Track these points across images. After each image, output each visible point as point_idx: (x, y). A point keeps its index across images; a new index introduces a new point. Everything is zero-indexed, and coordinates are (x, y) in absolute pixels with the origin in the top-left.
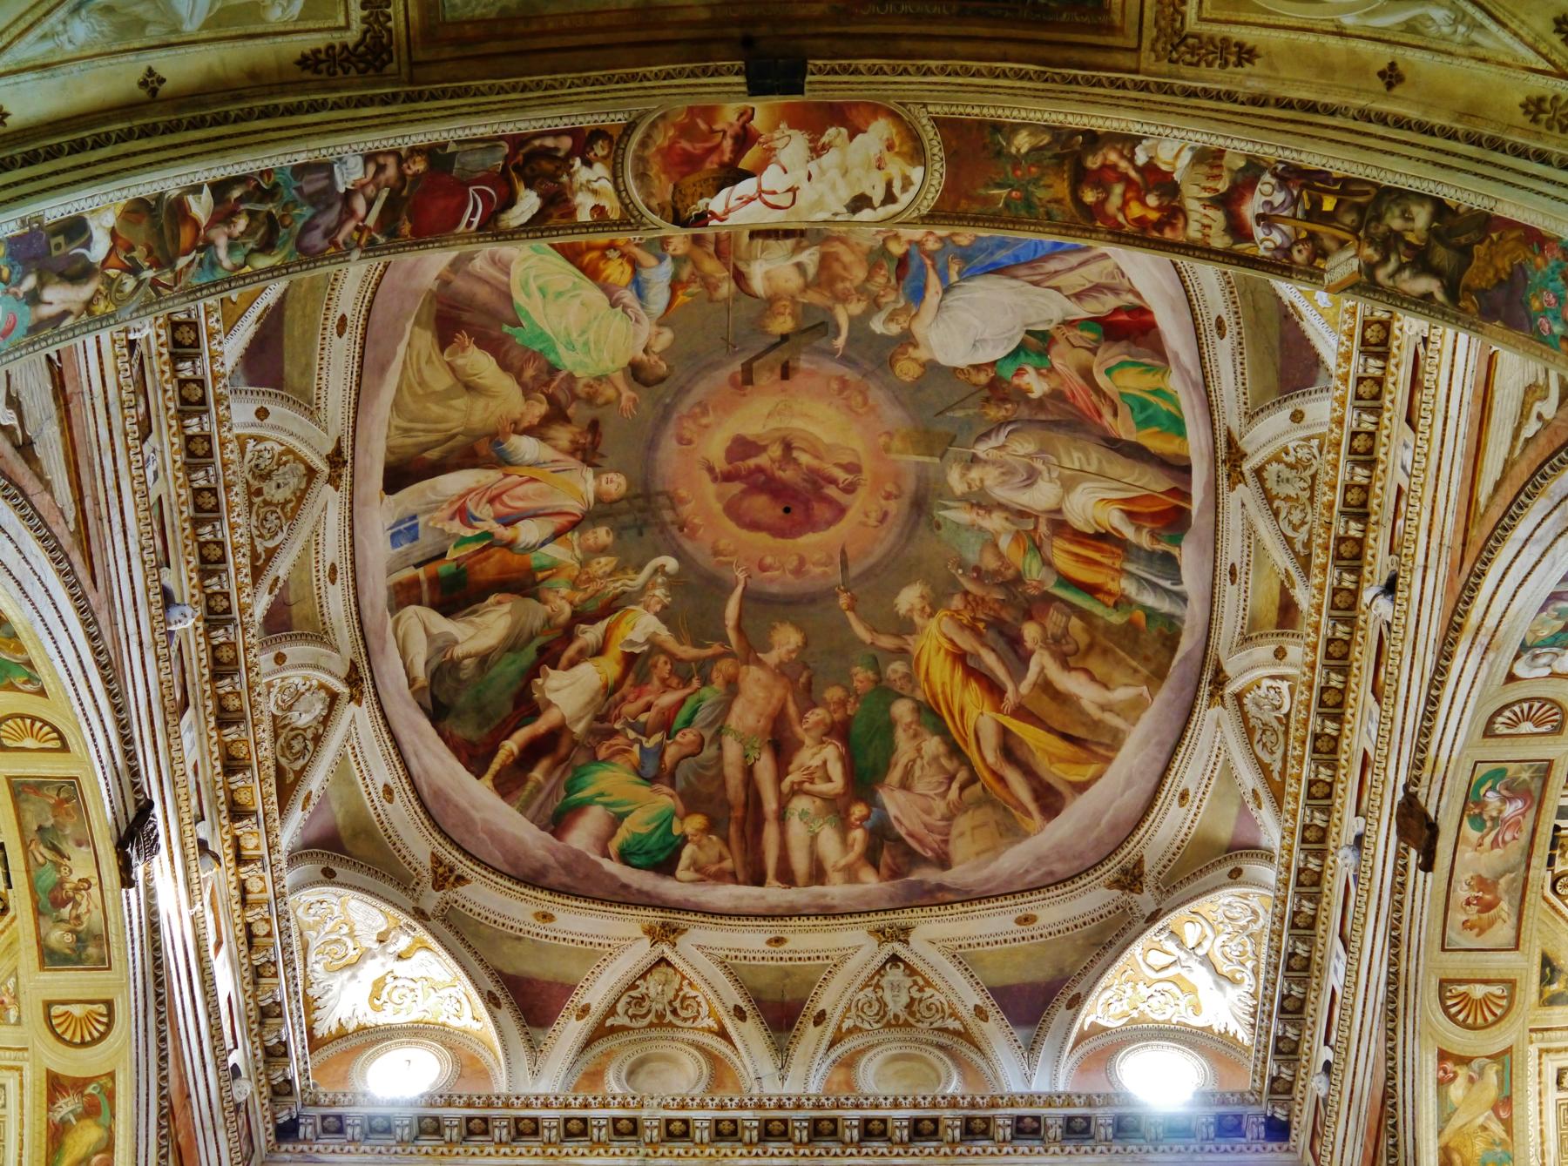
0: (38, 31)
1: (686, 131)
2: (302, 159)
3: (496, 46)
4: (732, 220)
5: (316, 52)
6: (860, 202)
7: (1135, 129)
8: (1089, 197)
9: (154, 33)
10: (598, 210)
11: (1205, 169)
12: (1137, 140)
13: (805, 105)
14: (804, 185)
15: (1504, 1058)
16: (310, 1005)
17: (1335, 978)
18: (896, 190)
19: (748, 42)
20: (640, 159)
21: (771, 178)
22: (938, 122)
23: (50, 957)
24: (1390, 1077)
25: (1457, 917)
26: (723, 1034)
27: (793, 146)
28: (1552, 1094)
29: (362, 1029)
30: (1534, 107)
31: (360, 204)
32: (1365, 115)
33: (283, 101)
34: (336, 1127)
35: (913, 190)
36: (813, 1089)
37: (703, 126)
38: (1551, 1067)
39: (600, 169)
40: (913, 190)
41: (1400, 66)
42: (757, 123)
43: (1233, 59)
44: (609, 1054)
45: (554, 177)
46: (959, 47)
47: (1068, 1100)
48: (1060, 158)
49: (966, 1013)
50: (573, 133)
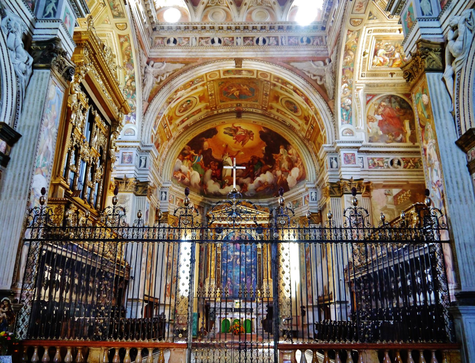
15: (359, 31)
16: (154, 3)
17: (336, 7)
23: (114, 16)
24: (340, 31)
25: (355, 8)
26: (228, 7)
28: (367, 34)
29: (164, 7)
34: (163, 28)
36: (244, 20)
38: (367, 30)
44: (208, 11)
47: (288, 23)
49: (272, 3)
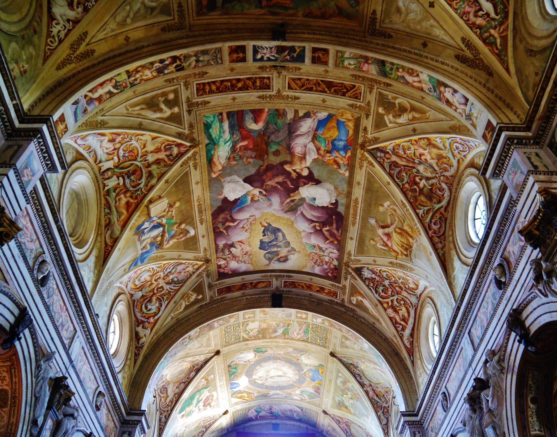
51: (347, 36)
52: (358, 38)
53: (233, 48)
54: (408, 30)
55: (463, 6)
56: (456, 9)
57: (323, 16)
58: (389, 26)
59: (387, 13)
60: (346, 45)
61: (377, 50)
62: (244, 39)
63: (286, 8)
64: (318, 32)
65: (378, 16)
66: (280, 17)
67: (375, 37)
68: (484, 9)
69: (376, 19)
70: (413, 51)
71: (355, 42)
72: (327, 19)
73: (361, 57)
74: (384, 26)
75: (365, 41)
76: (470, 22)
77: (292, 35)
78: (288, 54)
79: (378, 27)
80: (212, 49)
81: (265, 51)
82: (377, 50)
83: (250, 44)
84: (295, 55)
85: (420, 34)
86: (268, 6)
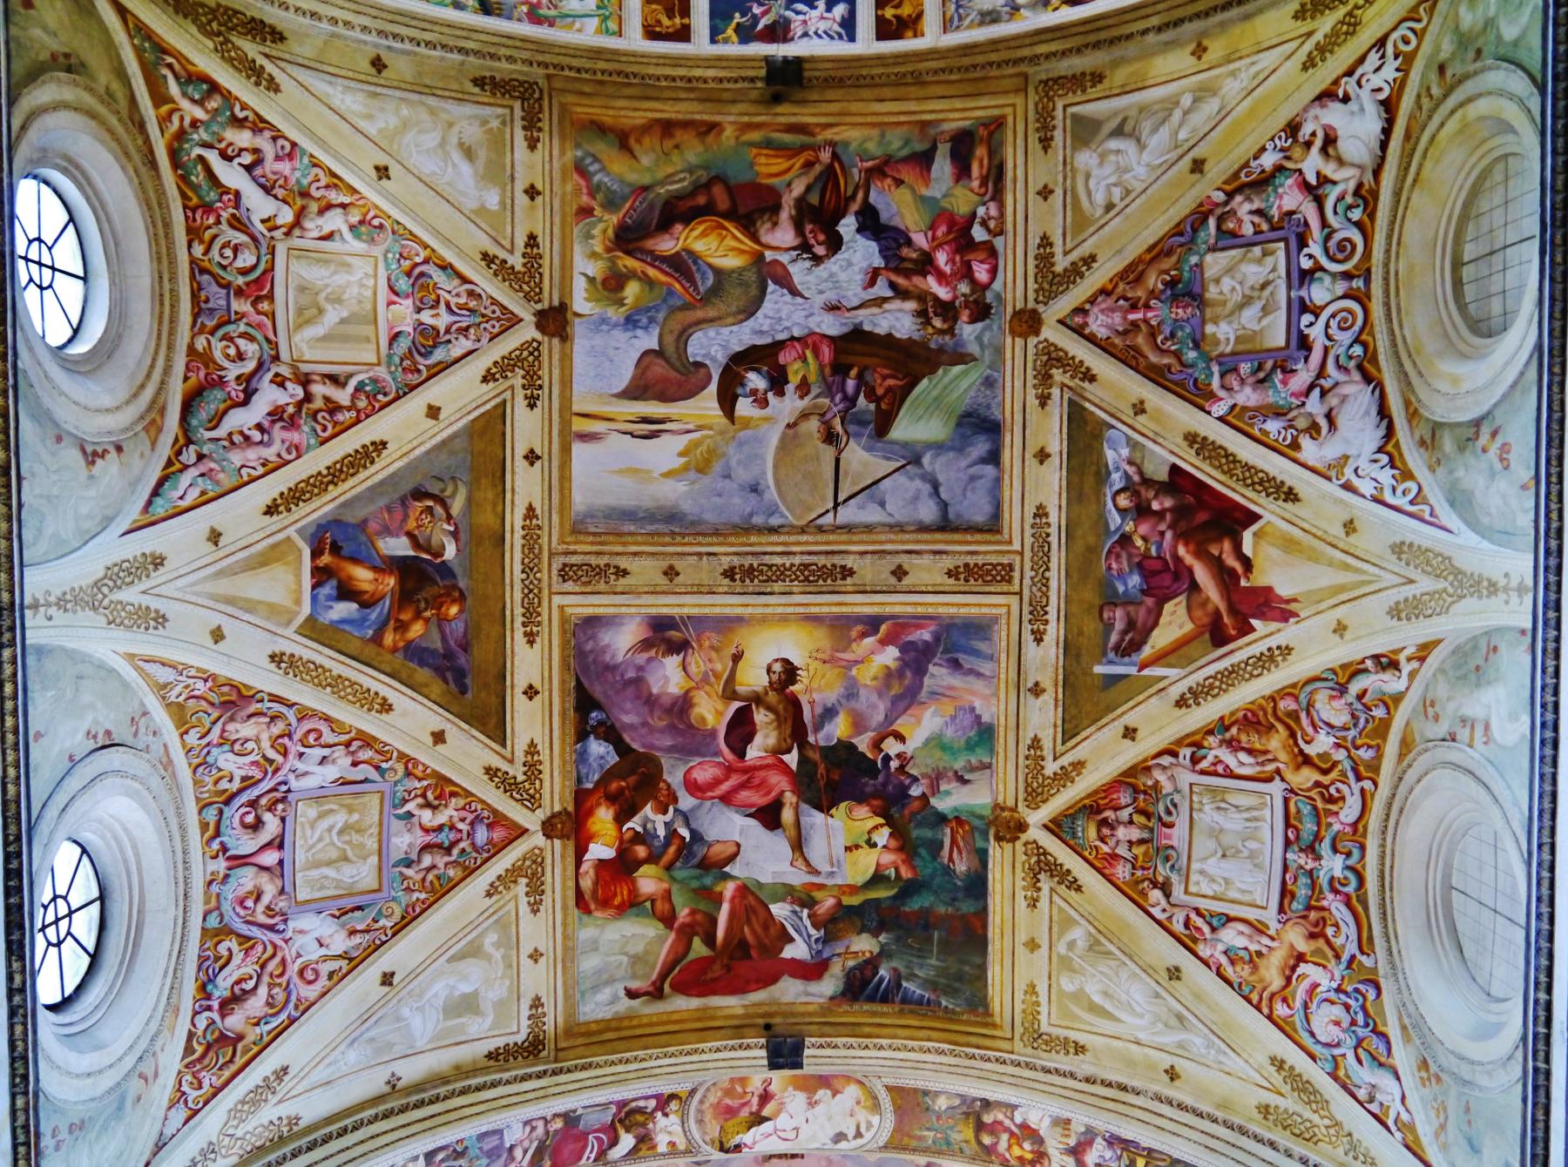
0: (327, 1061)
1: (729, 1092)
2: (484, 1129)
3: (610, 1035)
4: (757, 1148)
5: (497, 1049)
6: (840, 1137)
7: (1014, 1101)
8: (987, 1140)
9: (398, 1050)
10: (672, 1144)
11: (1059, 1130)
12: (1016, 1107)
13: (805, 1077)
14: (804, 1126)
18: (863, 1130)
19: (768, 1027)
20: (700, 1111)
21: (782, 1121)
22: (889, 1088)
27: (796, 1101)
30: (1265, 1110)
31: (518, 1153)
32: (1158, 1098)
33: (474, 1082)
35: (873, 1130)
37: (739, 1089)
39: (674, 1119)
40: (873, 1130)
41: (1177, 1068)
42: (773, 1088)
43: (1072, 1050)
45: (644, 1125)
46: (900, 1032)
48: (967, 1114)
50: (657, 1097)
51: (599, 76)
52: (567, 73)
53: (910, 33)
54: (432, 101)
55: (298, 174)
56: (315, 165)
57: (667, 128)
58: (488, 111)
59: (498, 143)
60: (597, 53)
61: (510, 42)
62: (880, 59)
63: (767, 144)
64: (679, 84)
65: (520, 135)
66: (782, 120)
67: (521, 78)
68: (242, 170)
69: (524, 128)
70: (407, 46)
71: (575, 62)
72: (658, 121)
73: (551, 23)
74: (500, 111)
75: (546, 66)
76: (267, 134)
77: (751, 73)
78: (756, 19)
79: (517, 105)
80: (969, 27)
81: (823, 26)
82: (510, 42)
83: (866, 43)
84: (737, 18)
85: (398, 93)
86: (816, 148)
